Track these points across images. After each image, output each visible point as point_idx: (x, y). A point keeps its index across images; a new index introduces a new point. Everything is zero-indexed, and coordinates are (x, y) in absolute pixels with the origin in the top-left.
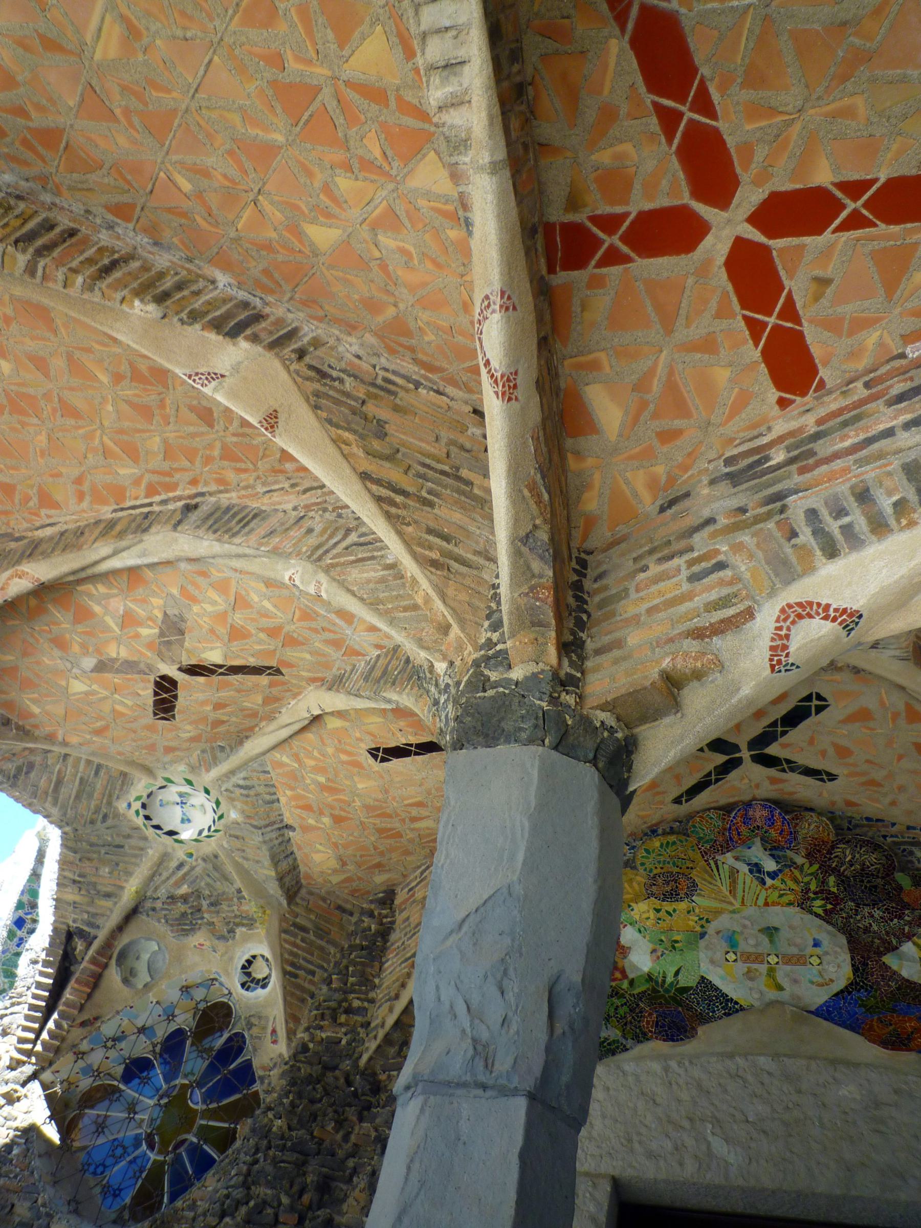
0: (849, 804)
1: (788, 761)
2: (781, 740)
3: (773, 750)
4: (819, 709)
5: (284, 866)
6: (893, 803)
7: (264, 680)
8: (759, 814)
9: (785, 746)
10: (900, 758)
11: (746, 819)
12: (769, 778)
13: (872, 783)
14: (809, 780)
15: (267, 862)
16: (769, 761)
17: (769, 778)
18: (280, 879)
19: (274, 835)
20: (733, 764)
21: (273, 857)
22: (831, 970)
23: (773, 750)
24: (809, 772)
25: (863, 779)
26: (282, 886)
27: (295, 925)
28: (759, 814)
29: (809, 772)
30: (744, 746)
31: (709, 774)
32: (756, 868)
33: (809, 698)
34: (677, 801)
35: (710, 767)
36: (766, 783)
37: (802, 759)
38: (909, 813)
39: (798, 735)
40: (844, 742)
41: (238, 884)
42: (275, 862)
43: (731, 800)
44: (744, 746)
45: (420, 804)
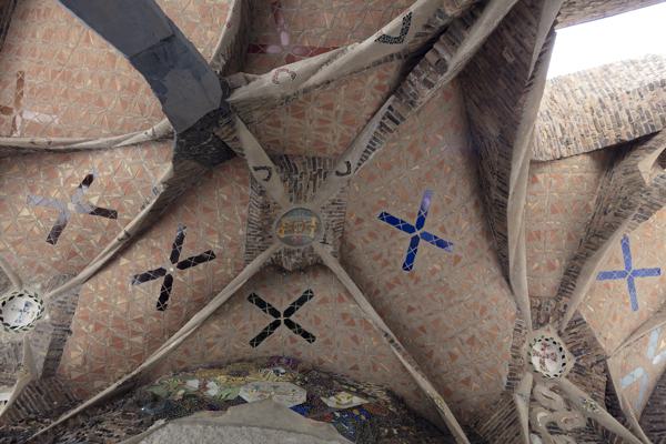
0: (321, 362)
1: (298, 326)
2: (297, 312)
3: (293, 318)
4: (311, 297)
5: (53, 354)
6: (335, 357)
7: (106, 221)
8: (283, 361)
9: (297, 316)
10: (338, 321)
11: (278, 361)
12: (291, 337)
13: (328, 342)
14: (304, 341)
15: (46, 346)
16: (290, 324)
17: (291, 337)
18: (47, 360)
19: (59, 332)
20: (276, 325)
21: (51, 345)
22: (297, 397)
23: (293, 318)
24: (306, 335)
25: (325, 339)
26: (45, 364)
27: (37, 388)
28: (283, 361)
29: (306, 335)
30: (282, 313)
31: (266, 329)
32: (277, 372)
33: (307, 292)
34: (252, 343)
35: (267, 324)
36: (288, 341)
37: (305, 327)
38: (342, 363)
39: (301, 310)
40: (318, 315)
41: (22, 362)
42: (51, 349)
43: (275, 353)
44: (282, 313)
45: (140, 321)
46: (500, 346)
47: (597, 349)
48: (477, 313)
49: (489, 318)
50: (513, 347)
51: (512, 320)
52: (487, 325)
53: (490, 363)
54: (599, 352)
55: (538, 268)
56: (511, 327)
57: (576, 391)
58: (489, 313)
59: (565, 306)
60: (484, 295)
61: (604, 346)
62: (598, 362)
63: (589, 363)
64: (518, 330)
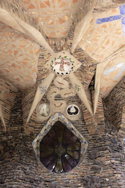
46: (31, 67)
47: (91, 61)
48: (13, 54)
49: (21, 55)
50: (38, 66)
51: (37, 53)
52: (20, 59)
53: (26, 74)
54: (93, 62)
55: (52, 23)
56: (36, 57)
57: (75, 81)
58: (20, 53)
59: (71, 43)
60: (14, 46)
61: (95, 59)
62: (93, 65)
63: (89, 65)
64: (42, 57)
